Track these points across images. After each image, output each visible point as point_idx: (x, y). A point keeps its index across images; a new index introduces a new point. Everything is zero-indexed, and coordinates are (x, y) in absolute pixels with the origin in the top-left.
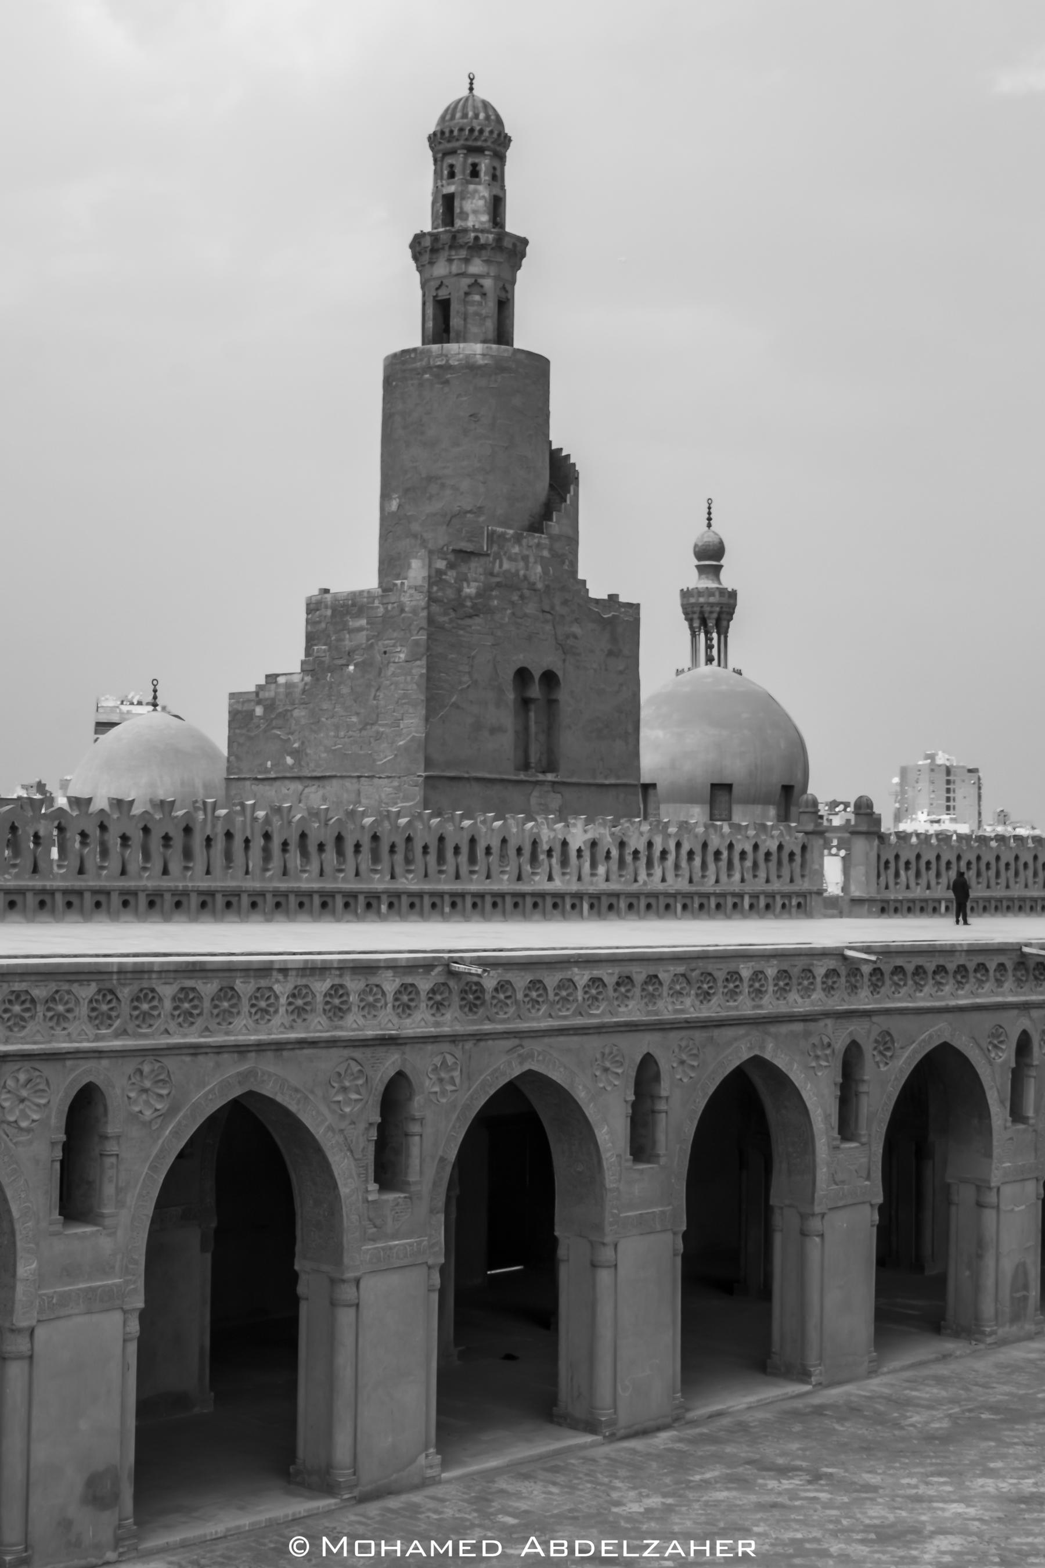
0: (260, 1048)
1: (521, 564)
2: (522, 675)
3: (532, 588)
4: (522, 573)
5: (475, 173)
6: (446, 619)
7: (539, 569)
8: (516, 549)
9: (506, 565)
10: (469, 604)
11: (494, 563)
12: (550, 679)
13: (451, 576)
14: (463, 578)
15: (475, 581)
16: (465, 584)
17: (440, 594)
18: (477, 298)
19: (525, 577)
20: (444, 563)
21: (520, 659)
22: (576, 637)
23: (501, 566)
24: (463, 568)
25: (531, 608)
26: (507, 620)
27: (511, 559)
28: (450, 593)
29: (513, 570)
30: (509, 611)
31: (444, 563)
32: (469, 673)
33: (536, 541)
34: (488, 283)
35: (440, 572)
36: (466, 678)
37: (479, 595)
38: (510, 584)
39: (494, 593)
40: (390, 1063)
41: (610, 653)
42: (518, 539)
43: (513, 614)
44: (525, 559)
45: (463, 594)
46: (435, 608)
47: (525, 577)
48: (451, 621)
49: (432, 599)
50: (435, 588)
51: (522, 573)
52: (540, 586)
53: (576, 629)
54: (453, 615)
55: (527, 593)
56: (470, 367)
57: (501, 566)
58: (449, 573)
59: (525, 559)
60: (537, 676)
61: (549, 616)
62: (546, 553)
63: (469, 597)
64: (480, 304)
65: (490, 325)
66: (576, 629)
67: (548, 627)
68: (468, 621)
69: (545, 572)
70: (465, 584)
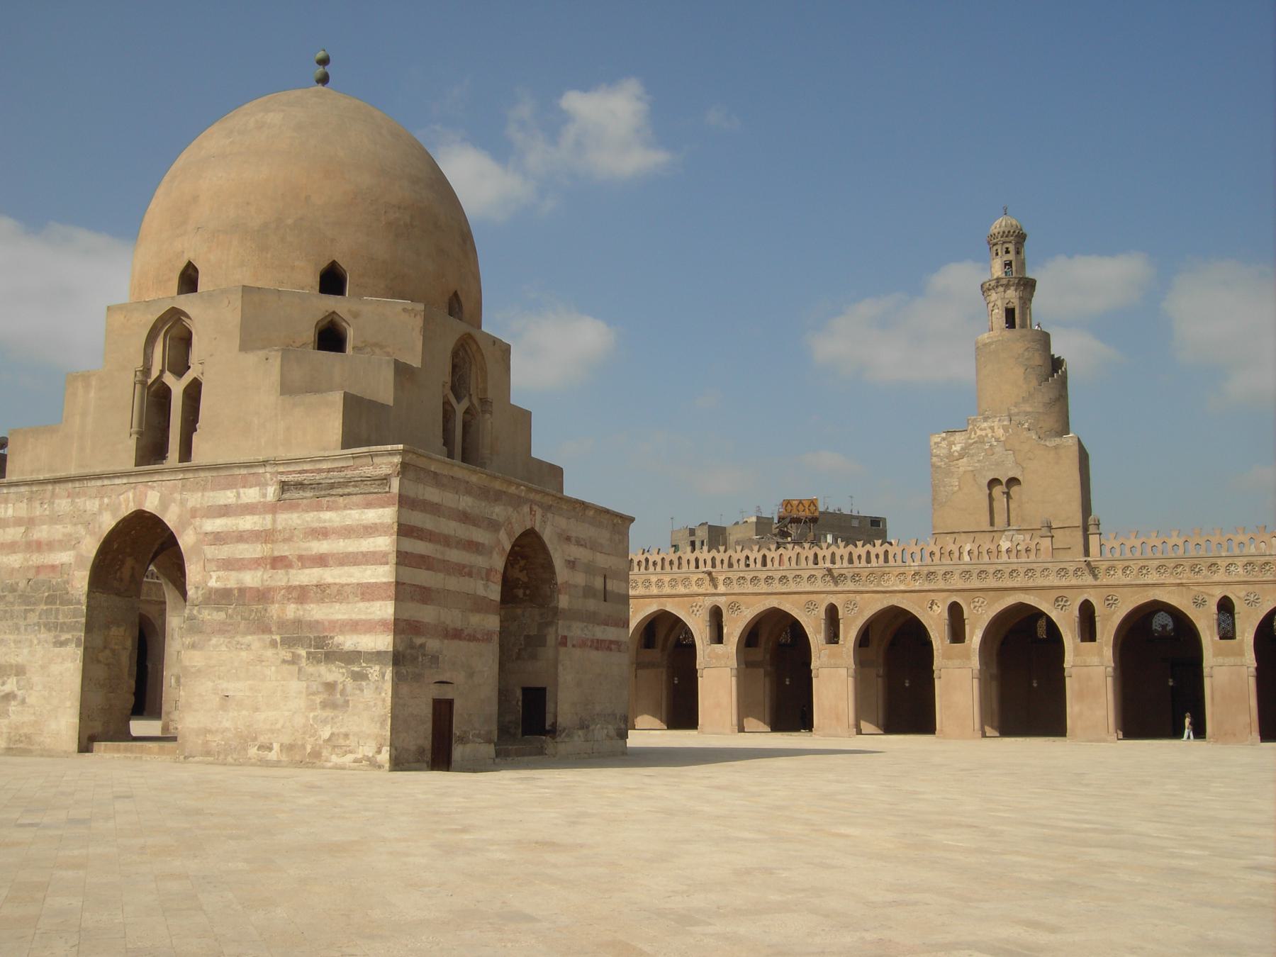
2: (993, 482)
3: (997, 440)
7: (1001, 431)
8: (985, 425)
9: (979, 433)
12: (1013, 481)
13: (944, 444)
14: (951, 444)
25: (999, 449)
28: (943, 452)
37: (962, 449)
38: (981, 440)
42: (986, 419)
44: (992, 428)
46: (935, 459)
59: (992, 428)
60: (1004, 481)
67: (1011, 458)
69: (1006, 429)
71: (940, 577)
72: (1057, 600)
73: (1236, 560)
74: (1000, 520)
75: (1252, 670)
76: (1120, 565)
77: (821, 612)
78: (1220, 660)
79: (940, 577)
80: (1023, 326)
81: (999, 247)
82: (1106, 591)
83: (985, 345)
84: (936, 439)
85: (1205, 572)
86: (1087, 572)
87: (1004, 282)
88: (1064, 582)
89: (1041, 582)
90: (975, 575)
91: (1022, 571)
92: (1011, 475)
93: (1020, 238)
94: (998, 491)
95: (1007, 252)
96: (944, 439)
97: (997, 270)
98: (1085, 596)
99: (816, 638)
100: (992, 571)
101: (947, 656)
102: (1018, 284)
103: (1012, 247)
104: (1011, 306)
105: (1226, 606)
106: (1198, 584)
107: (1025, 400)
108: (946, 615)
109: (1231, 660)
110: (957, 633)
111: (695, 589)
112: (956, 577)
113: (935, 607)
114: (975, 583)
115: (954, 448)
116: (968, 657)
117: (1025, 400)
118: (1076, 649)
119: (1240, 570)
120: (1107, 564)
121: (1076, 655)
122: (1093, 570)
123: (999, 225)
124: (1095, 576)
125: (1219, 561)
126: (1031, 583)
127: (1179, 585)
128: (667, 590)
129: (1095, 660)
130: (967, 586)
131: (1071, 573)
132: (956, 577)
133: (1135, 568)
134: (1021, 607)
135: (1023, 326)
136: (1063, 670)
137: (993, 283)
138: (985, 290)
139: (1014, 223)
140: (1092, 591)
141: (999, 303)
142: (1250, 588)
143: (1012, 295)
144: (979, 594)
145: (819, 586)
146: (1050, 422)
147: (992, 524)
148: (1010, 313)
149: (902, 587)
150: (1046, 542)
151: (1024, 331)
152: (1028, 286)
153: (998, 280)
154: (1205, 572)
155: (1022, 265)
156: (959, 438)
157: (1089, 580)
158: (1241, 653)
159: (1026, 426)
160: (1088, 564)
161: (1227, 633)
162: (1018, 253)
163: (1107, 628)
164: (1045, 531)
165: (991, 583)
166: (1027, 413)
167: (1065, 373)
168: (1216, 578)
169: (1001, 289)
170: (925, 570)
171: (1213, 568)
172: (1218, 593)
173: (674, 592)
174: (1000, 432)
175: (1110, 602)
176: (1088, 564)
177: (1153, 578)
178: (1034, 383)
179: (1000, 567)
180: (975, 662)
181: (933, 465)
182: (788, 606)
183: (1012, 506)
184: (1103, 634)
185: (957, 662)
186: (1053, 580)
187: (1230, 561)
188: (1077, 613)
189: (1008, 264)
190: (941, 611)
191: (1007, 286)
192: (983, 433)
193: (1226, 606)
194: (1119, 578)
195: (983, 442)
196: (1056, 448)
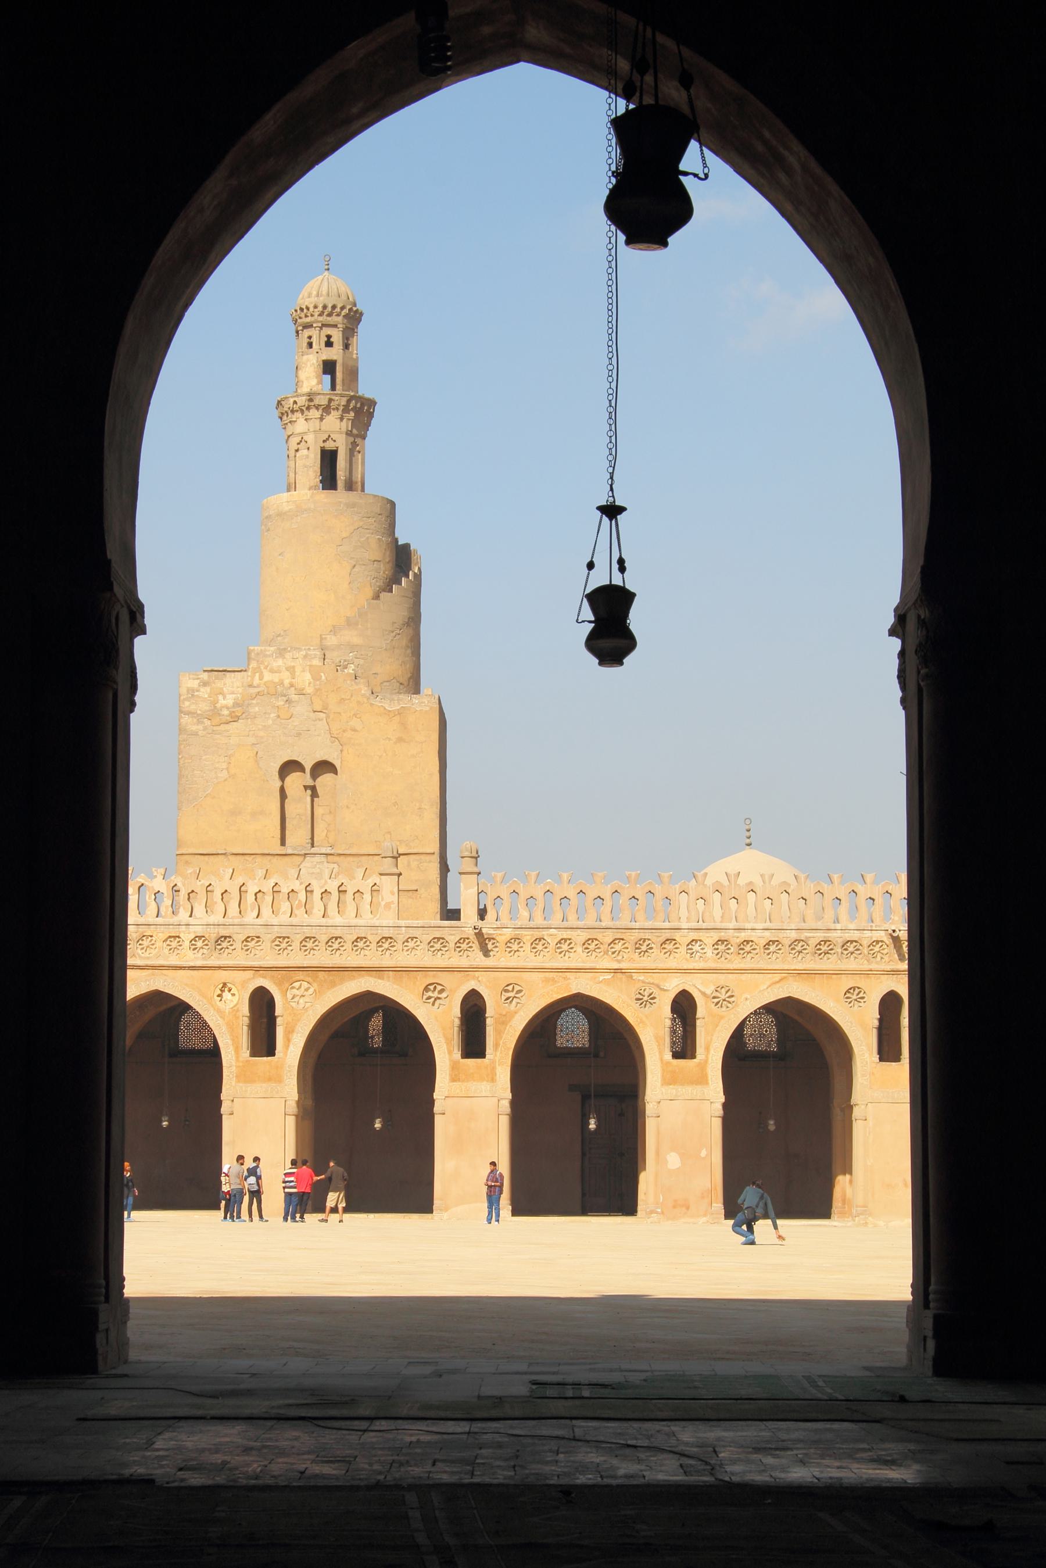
1: (288, 673)
2: (290, 767)
3: (301, 693)
4: (287, 682)
5: (310, 345)
6: (201, 727)
7: (308, 676)
9: (268, 677)
10: (226, 712)
11: (253, 677)
12: (324, 767)
13: (204, 692)
15: (233, 693)
16: (221, 697)
17: (193, 707)
18: (305, 452)
19: (292, 685)
20: (197, 682)
22: (354, 730)
23: (261, 678)
24: (219, 684)
25: (301, 709)
26: (270, 722)
27: (272, 671)
28: (203, 707)
29: (277, 680)
30: (272, 715)
31: (197, 682)
32: (227, 769)
33: (304, 653)
34: (310, 438)
35: (191, 691)
36: (225, 772)
37: (236, 704)
39: (254, 702)
41: (400, 740)
42: (281, 653)
43: (278, 716)
44: (291, 670)
45: (218, 705)
46: (186, 719)
47: (292, 685)
48: (205, 729)
50: (187, 703)
51: (287, 682)
52: (309, 690)
53: (355, 723)
54: (207, 722)
55: (295, 697)
57: (261, 678)
58: (202, 690)
59: (291, 670)
60: (308, 768)
61: (323, 715)
62: (317, 662)
63: (228, 708)
64: (307, 457)
66: (355, 723)
68: (226, 727)
69: (316, 678)
70: (221, 697)
71: (238, 945)
72: (426, 989)
73: (701, 935)
74: (297, 836)
75: (718, 1109)
76: (528, 936)
78: (671, 1090)
79: (238, 945)
81: (314, 333)
82: (504, 978)
83: (281, 515)
84: (189, 682)
85: (656, 951)
86: (476, 946)
87: (323, 401)
88: (439, 961)
90: (296, 944)
91: (374, 939)
93: (354, 318)
94: (295, 782)
95: (329, 344)
96: (205, 684)
97: (311, 379)
98: (471, 985)
100: (324, 938)
101: (244, 1076)
102: (346, 409)
103: (337, 336)
104: (330, 445)
105: (684, 1008)
106: (645, 970)
107: (350, 623)
108: (245, 1010)
109: (688, 1091)
110: (263, 1040)
112: (266, 945)
113: (227, 995)
114: (296, 958)
115: (222, 702)
116: (276, 1078)
117: (350, 623)
118: (454, 1066)
119: (709, 952)
120: (508, 933)
121: (454, 1079)
122: (483, 942)
123: (319, 289)
124: (486, 953)
125: (677, 936)
126: (387, 961)
127: (616, 971)
129: (484, 1087)
130: (282, 961)
131: (452, 945)
132: (266, 945)
133: (552, 942)
135: (350, 486)
136: (432, 1102)
137: (302, 401)
138: (284, 412)
139: (343, 289)
140: (482, 976)
142: (722, 979)
143: (335, 428)
144: (300, 975)
146: (392, 666)
147: (283, 843)
148: (329, 458)
149: (174, 961)
150: (388, 884)
152: (362, 412)
153: (311, 397)
154: (656, 951)
155: (353, 374)
157: (476, 957)
158: (702, 1079)
159: (350, 670)
160: (479, 935)
161: (684, 1047)
162: (346, 346)
163: (503, 1039)
164: (387, 865)
165: (322, 957)
166: (352, 648)
167: (418, 577)
168: (672, 963)
169: (315, 414)
170: (213, 934)
171: (669, 946)
172: (674, 986)
174: (305, 679)
175: (511, 993)
176: (479, 935)
177: (578, 958)
178: (369, 592)
179: (337, 932)
180: (290, 1089)
181: (181, 730)
183: (318, 811)
184: (496, 1046)
185: (259, 1088)
187: (693, 935)
188: (457, 1011)
189: (329, 367)
191: (327, 409)
192: (276, 678)
193: (684, 1008)
194: (526, 957)
195: (276, 695)
196: (399, 713)
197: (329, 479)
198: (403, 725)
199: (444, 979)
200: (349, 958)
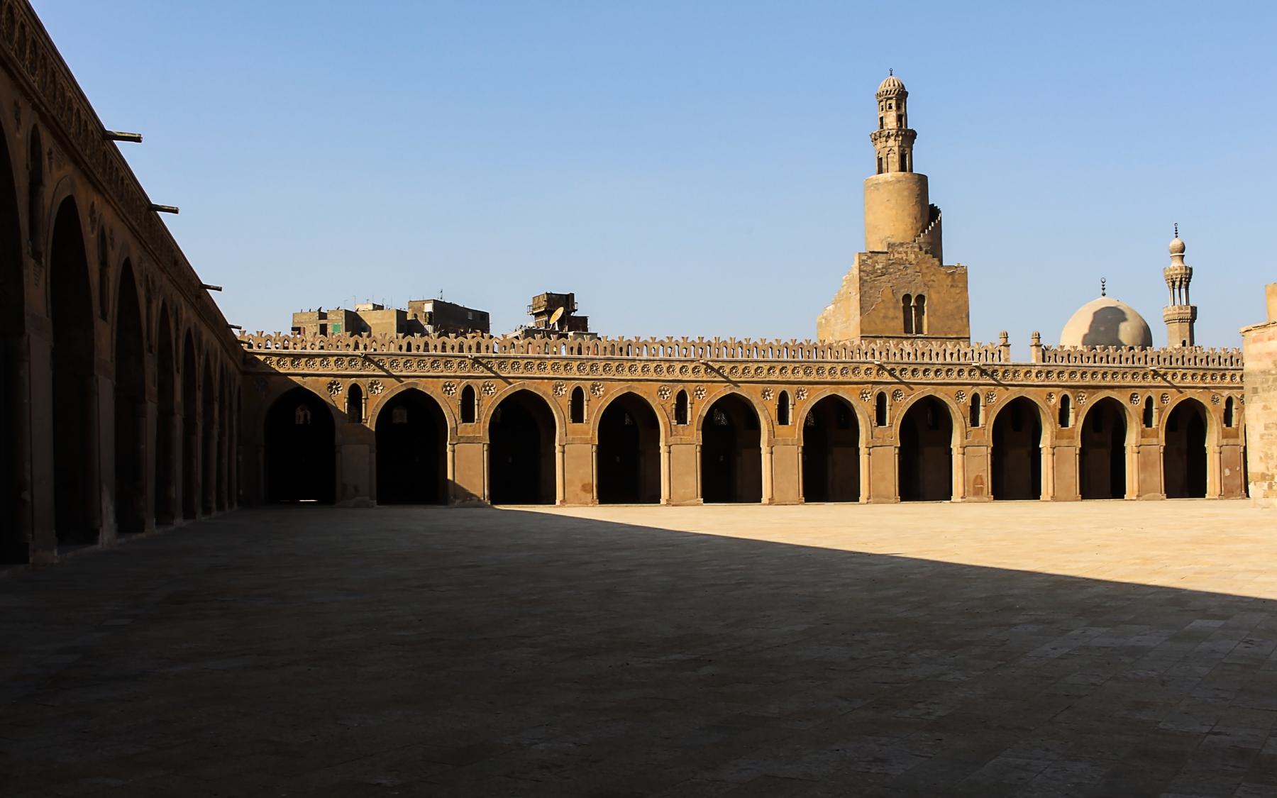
0: (632, 380)
13: (869, 262)
21: (904, 292)
28: (870, 268)
40: (680, 387)
49: (860, 271)
56: (887, 182)
65: (897, 166)
77: (967, 400)
80: (911, 170)
89: (1118, 381)
92: (920, 292)
99: (664, 420)
109: (1231, 441)
111: (862, 377)
128: (839, 378)
129: (1155, 441)
134: (1108, 401)
141: (896, 149)
145: (965, 378)
151: (907, 174)
156: (881, 258)
165: (1088, 381)
172: (1226, 393)
173: (845, 379)
177: (1188, 381)
182: (940, 394)
185: (1065, 442)
186: (1128, 381)
190: (1056, 400)
197: (903, 168)
198: (953, 280)
199: (1137, 391)
200: (1098, 381)
